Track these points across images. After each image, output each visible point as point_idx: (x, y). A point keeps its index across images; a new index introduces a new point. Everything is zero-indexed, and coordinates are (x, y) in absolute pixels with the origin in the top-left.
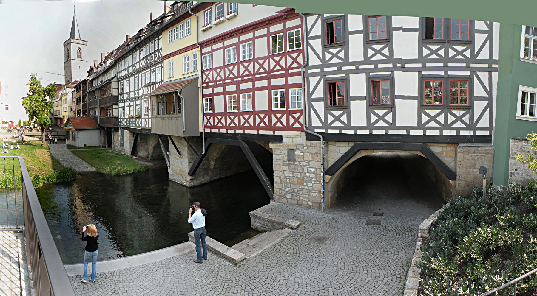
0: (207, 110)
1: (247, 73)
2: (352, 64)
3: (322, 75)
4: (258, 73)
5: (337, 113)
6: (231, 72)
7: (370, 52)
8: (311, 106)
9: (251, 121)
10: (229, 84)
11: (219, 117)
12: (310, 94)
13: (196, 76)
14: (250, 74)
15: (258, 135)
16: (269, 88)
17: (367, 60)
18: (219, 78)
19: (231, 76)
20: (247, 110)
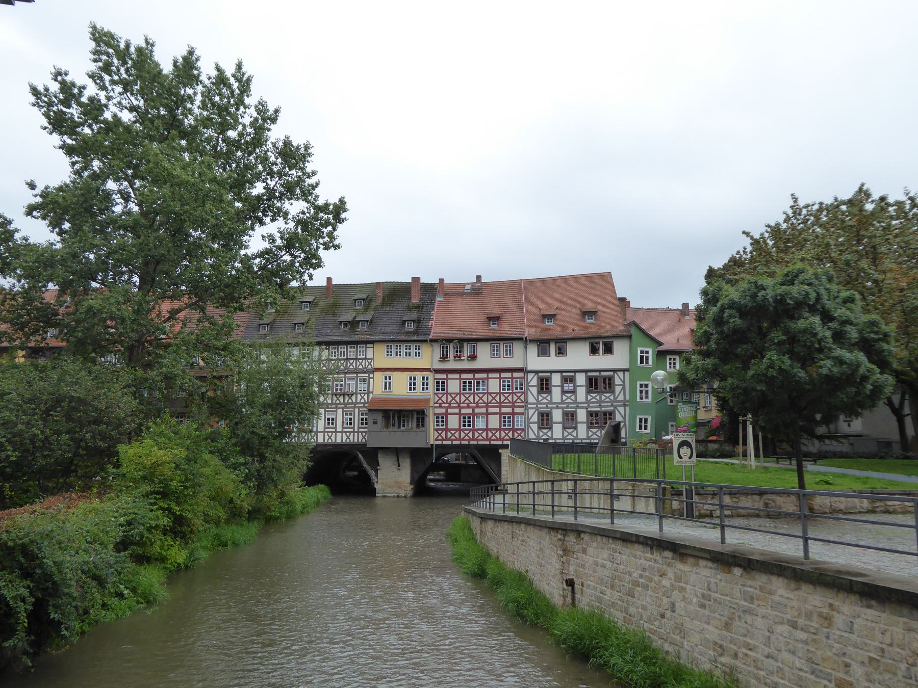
0: (437, 425)
1: (481, 401)
2: (554, 403)
3: (537, 409)
4: (490, 403)
5: (545, 431)
6: (467, 399)
7: (564, 398)
8: (529, 426)
9: (484, 435)
10: (464, 407)
11: (453, 432)
12: (529, 420)
13: (428, 397)
14: (484, 403)
15: (490, 444)
16: (500, 414)
17: (562, 402)
18: (453, 401)
19: (467, 401)
20: (480, 427)
